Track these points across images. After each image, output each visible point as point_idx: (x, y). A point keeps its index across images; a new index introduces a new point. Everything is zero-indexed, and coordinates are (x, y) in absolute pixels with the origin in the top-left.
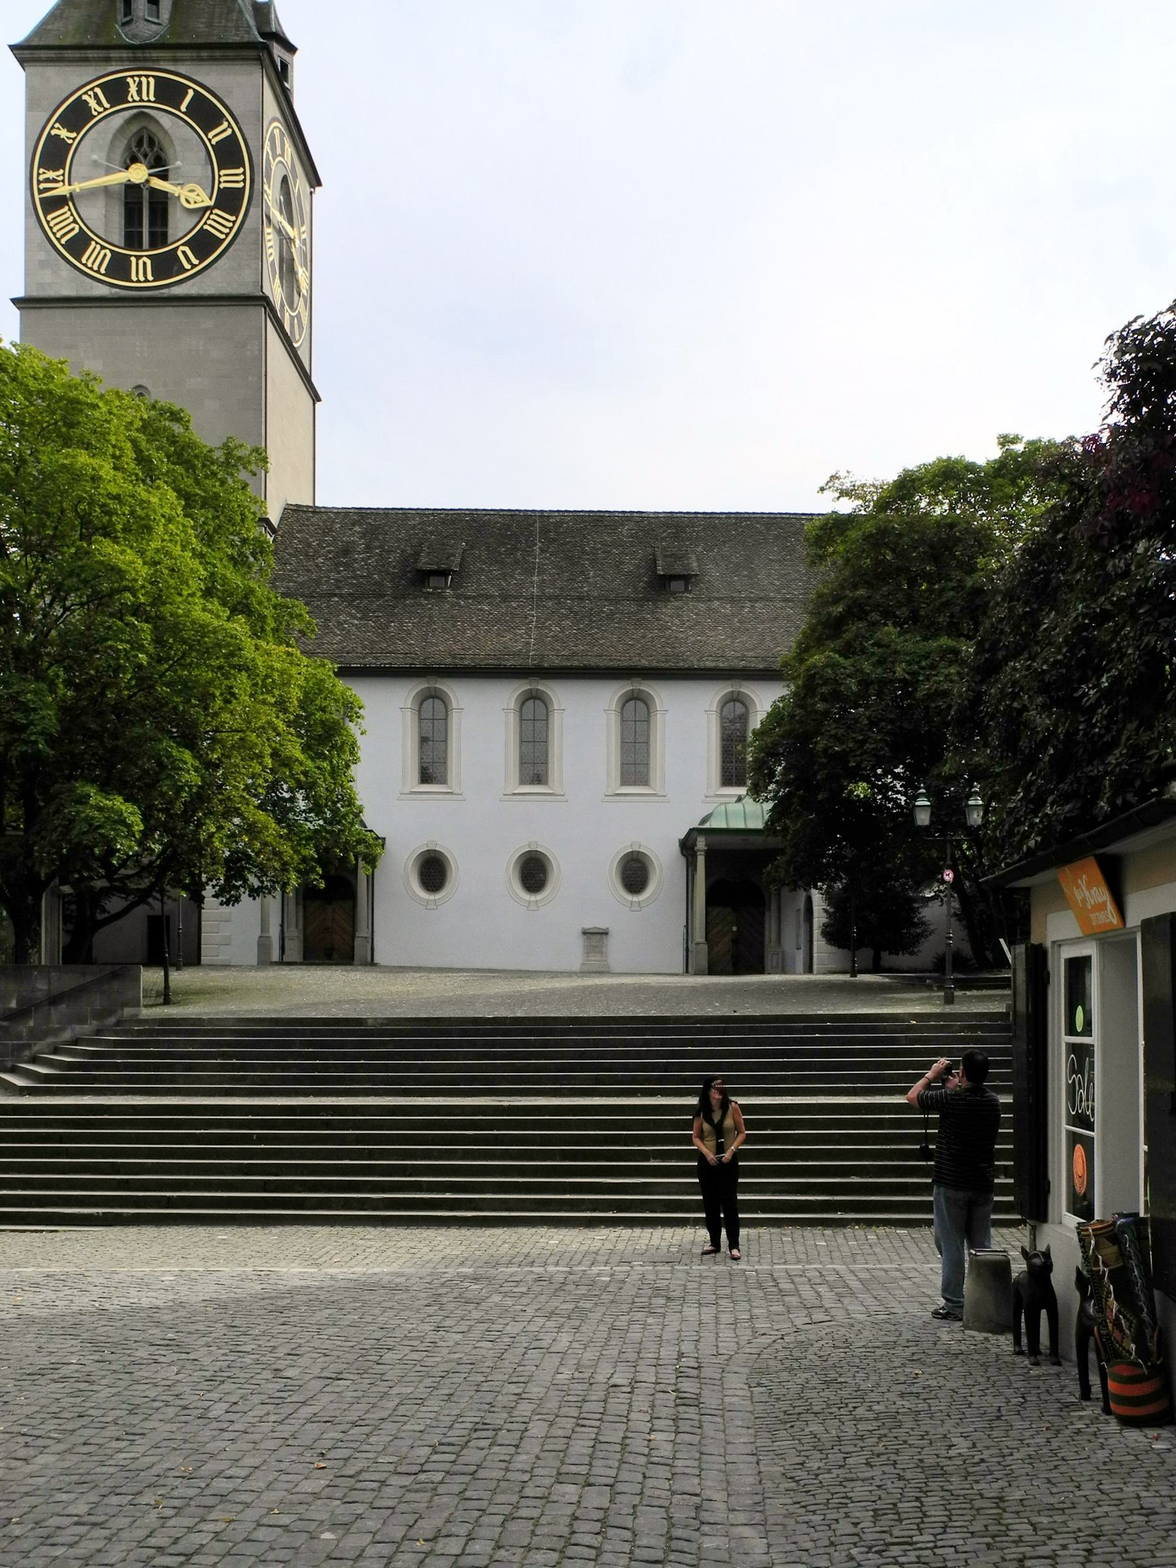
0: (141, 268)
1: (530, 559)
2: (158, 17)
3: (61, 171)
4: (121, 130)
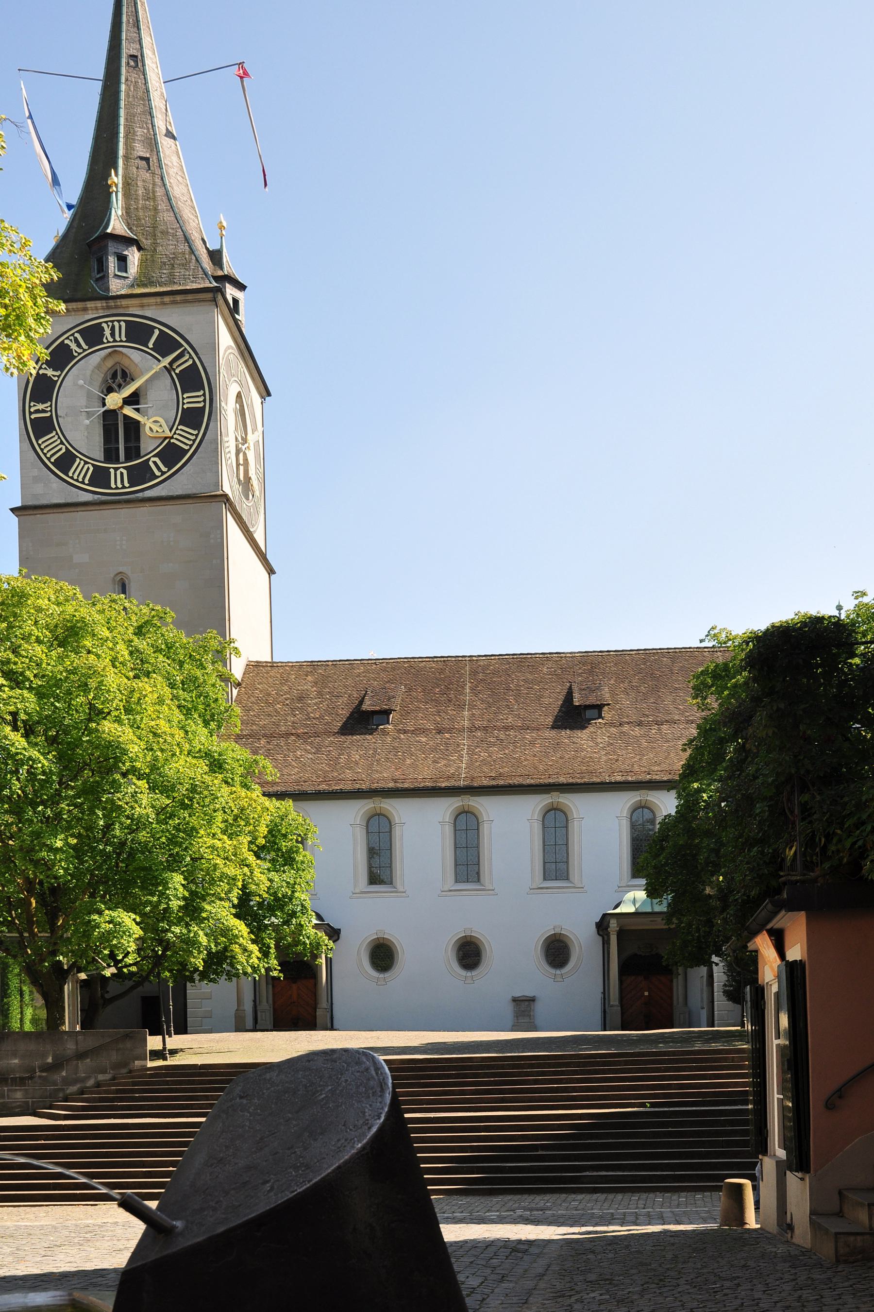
0: (119, 475)
1: (462, 697)
2: (126, 272)
4: (98, 367)
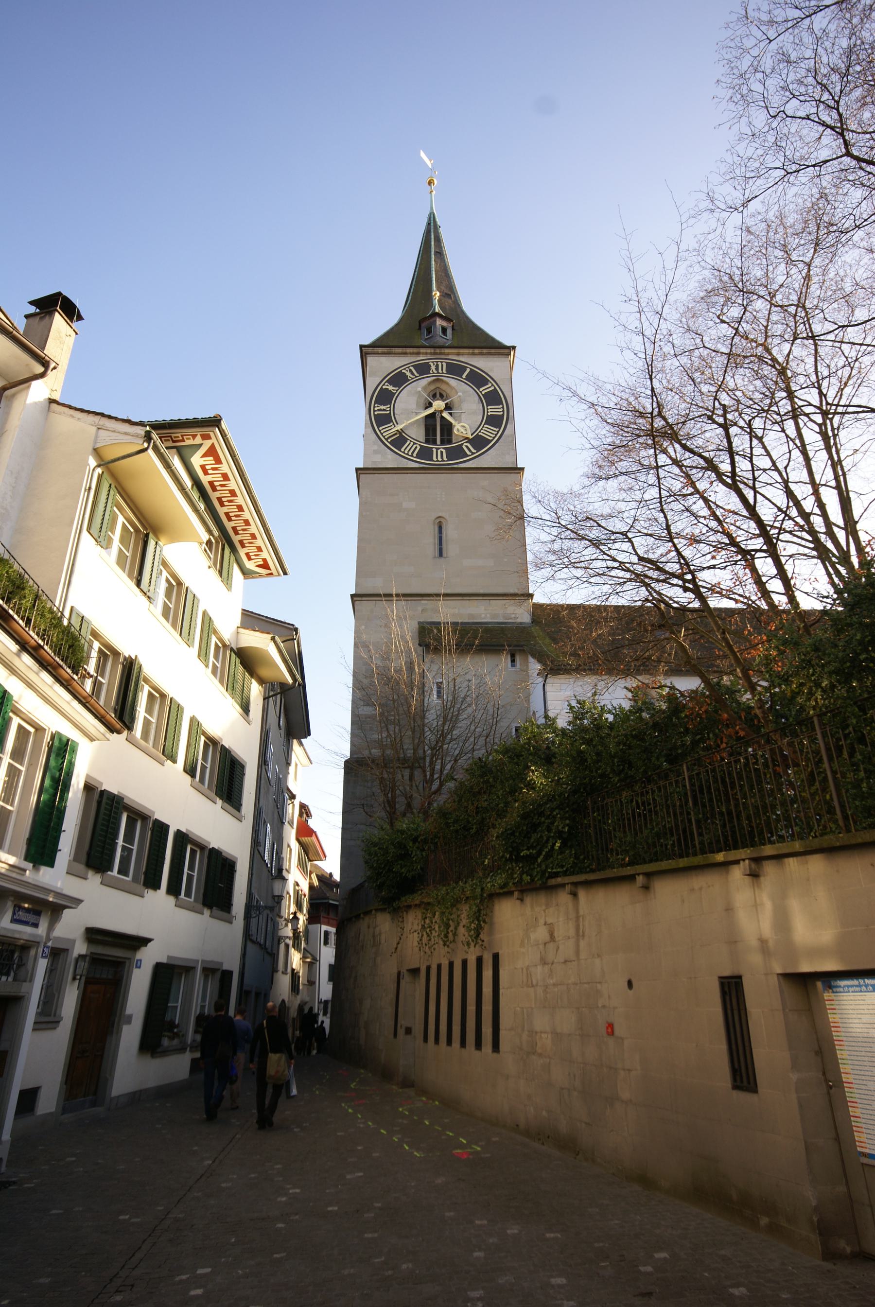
3: (389, 406)
4: (424, 388)
